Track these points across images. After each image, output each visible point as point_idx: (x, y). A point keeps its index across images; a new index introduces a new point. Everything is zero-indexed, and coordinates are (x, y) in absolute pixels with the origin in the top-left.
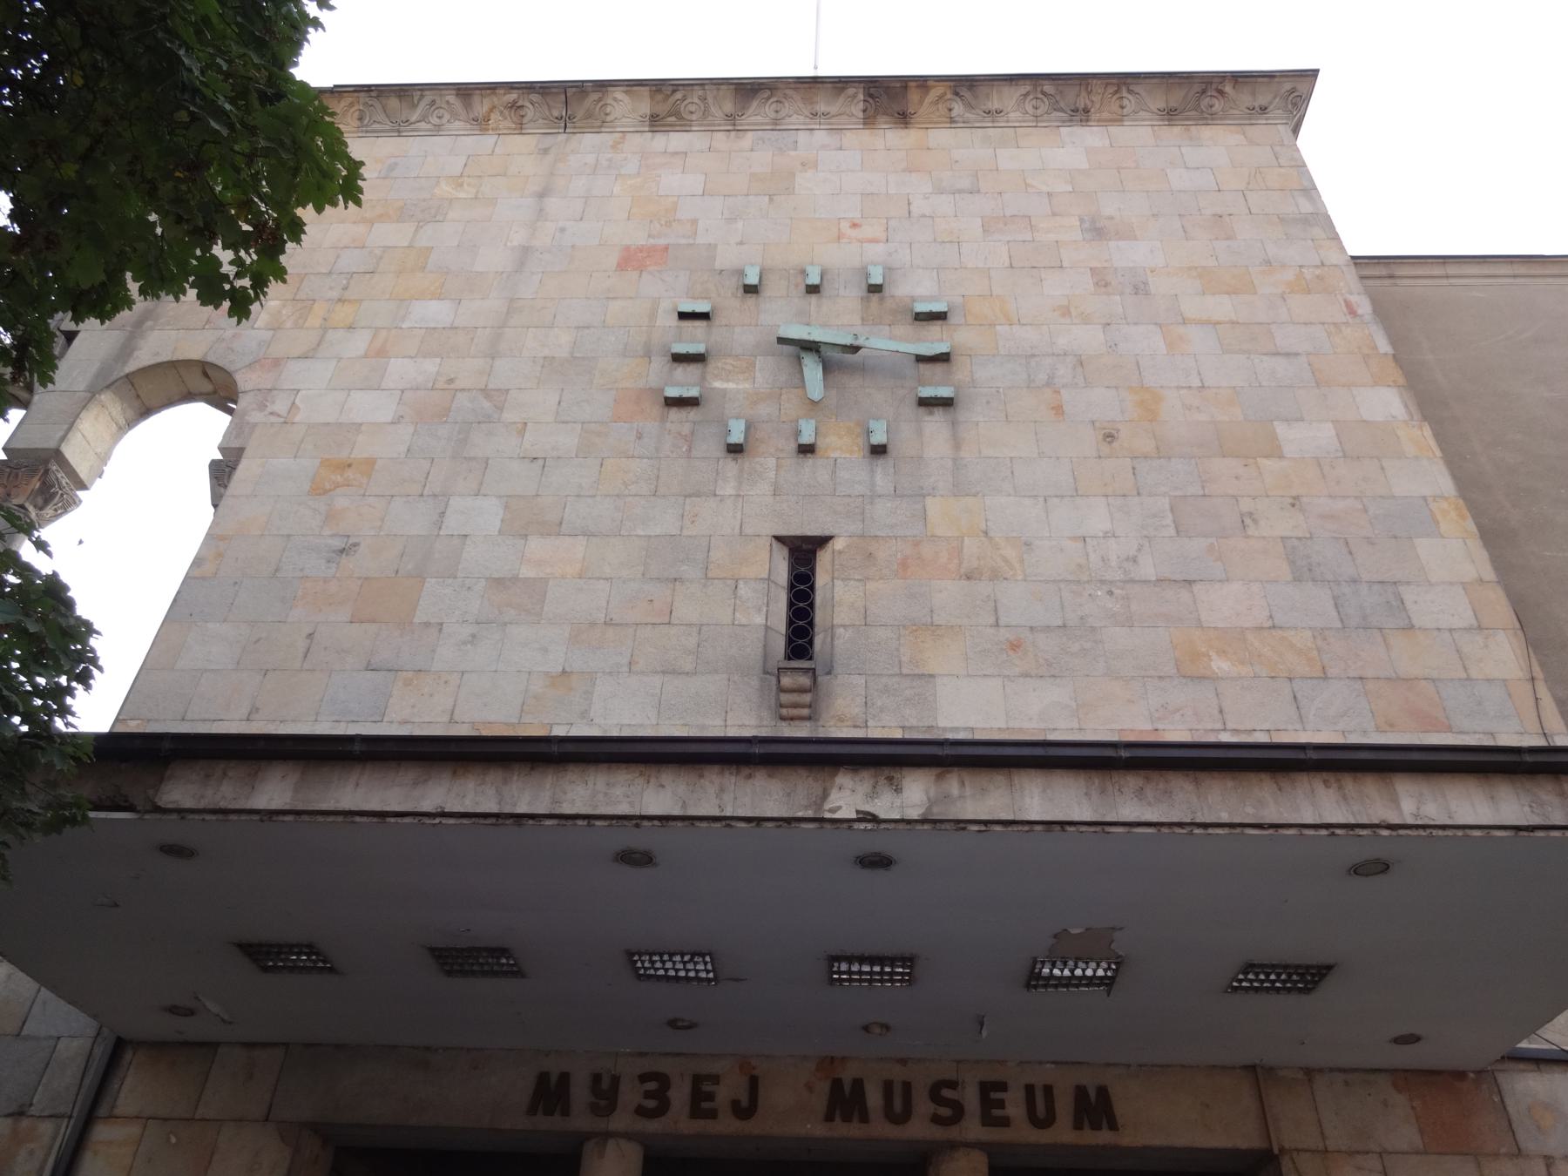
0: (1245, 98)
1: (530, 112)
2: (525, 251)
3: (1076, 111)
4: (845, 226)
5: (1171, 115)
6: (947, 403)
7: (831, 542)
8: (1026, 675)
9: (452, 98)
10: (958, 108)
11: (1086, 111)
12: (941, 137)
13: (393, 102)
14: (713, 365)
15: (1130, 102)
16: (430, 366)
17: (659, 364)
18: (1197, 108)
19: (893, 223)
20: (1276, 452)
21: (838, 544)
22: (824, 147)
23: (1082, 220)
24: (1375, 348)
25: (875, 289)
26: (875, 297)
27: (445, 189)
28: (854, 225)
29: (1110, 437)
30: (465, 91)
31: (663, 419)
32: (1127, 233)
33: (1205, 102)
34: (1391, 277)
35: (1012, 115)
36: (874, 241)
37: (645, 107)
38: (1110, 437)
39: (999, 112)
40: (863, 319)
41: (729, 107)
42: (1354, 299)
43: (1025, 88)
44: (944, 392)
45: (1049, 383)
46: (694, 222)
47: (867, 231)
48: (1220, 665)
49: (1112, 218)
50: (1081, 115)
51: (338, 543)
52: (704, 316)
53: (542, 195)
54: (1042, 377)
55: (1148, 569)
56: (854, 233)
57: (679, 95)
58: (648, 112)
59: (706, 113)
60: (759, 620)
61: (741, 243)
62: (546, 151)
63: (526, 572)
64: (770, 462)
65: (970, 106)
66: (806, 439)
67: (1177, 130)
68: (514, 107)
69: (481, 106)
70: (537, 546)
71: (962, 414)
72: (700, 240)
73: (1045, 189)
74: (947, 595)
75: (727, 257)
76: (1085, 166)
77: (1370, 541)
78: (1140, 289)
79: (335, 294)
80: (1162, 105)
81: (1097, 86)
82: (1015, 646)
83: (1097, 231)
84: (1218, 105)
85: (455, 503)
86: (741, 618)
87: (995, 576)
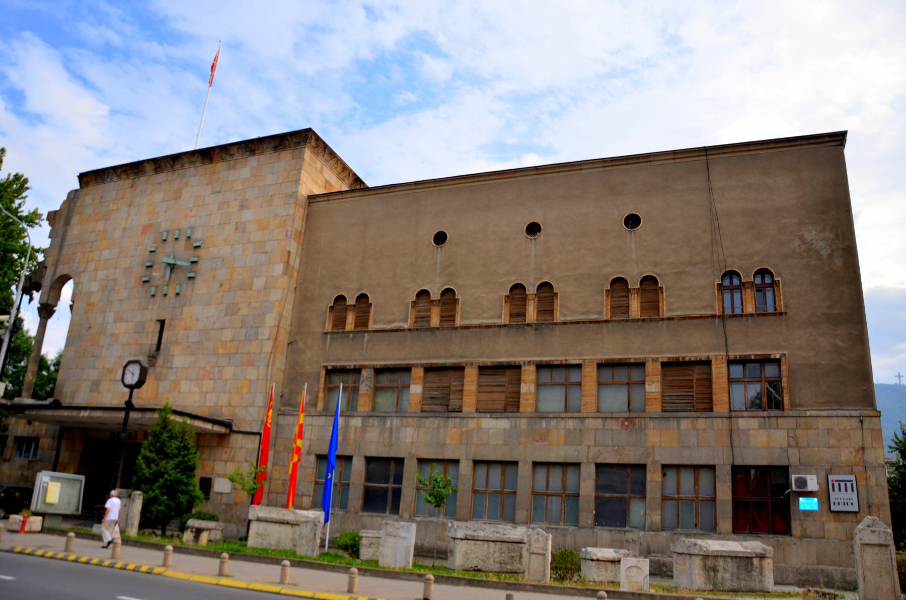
0: (295, 140)
1: (129, 172)
2: (125, 229)
3: (252, 151)
5: (275, 149)
6: (193, 278)
8: (189, 354)
9: (112, 171)
10: (224, 155)
11: (254, 151)
13: (100, 174)
14: (155, 267)
16: (105, 272)
17: (144, 268)
18: (281, 145)
20: (251, 289)
23: (240, 202)
24: (285, 248)
25: (189, 237)
29: (221, 285)
30: (115, 169)
31: (143, 287)
32: (248, 208)
33: (284, 143)
34: (328, 200)
35: (237, 155)
36: (193, 217)
37: (153, 166)
38: (221, 285)
39: (233, 154)
41: (171, 163)
42: (289, 228)
44: (192, 275)
45: (215, 268)
46: (158, 213)
48: (221, 351)
49: (247, 200)
50: (253, 152)
52: (154, 251)
53: (130, 206)
54: (214, 266)
55: (216, 326)
56: (190, 214)
57: (159, 162)
58: (153, 167)
59: (166, 167)
60: (150, 342)
61: (166, 221)
62: (132, 186)
63: (117, 332)
64: (158, 298)
65: (226, 154)
66: (165, 292)
67: (277, 153)
68: (125, 171)
69: (119, 172)
70: (119, 325)
72: (159, 221)
73: (236, 188)
74: (181, 333)
77: (259, 315)
78: (244, 231)
79: (89, 250)
80: (273, 145)
81: (255, 142)
82: (189, 347)
83: (242, 207)
84: (287, 143)
85: (108, 313)
86: (148, 342)
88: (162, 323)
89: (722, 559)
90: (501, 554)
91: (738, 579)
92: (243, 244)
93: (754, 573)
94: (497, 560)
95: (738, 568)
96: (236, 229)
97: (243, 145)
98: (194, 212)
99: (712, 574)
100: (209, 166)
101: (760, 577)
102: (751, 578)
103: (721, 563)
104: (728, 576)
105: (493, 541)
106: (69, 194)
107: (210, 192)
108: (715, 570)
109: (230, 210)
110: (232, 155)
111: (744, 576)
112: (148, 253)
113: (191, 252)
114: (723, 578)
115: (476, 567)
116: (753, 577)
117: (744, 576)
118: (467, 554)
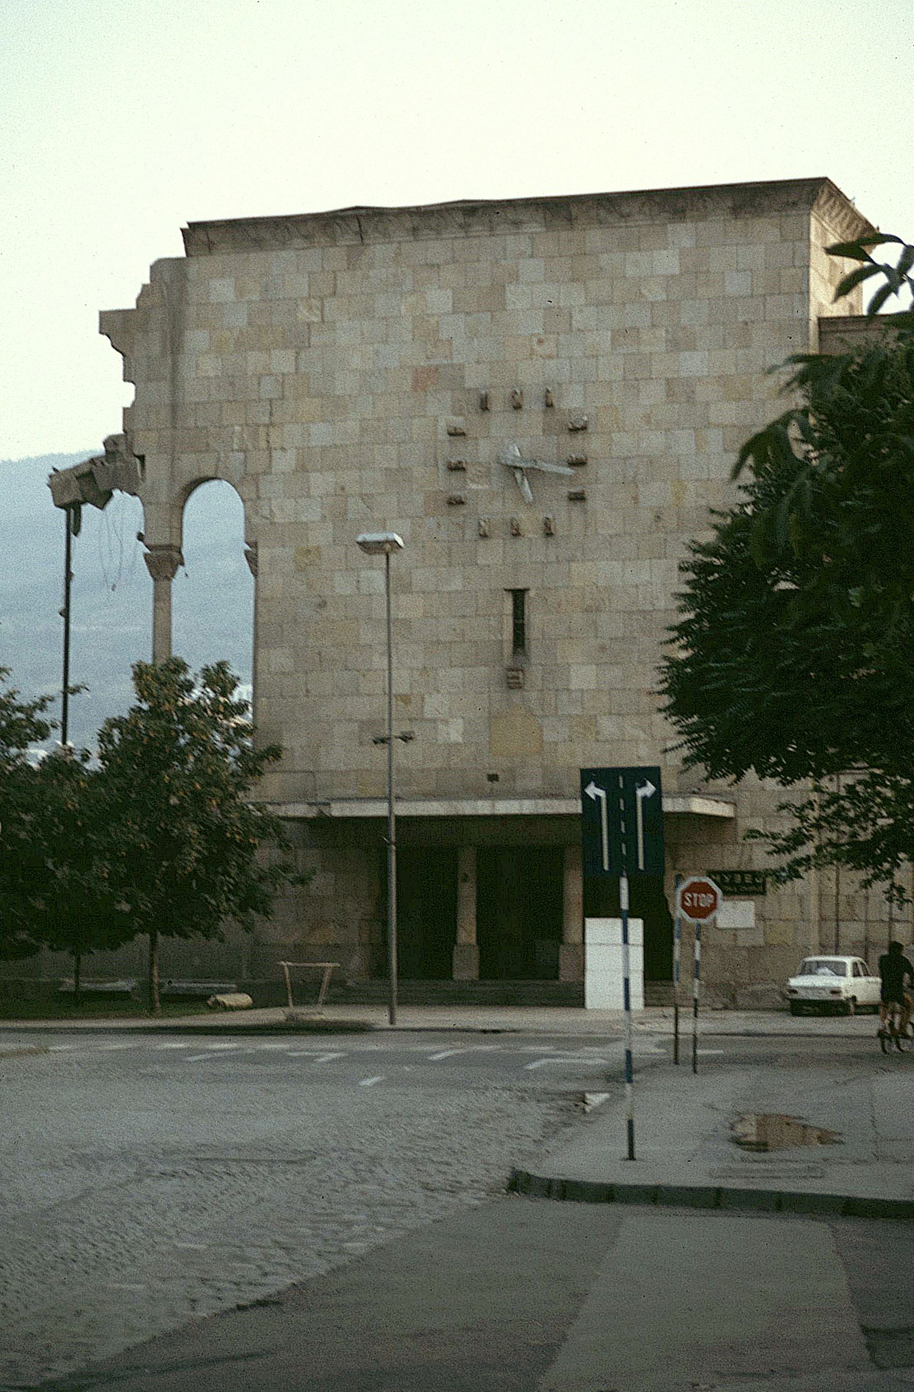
4: (535, 340)
5: (736, 211)
7: (527, 593)
10: (603, 213)
11: (684, 211)
12: (595, 237)
15: (710, 205)
16: (330, 477)
19: (561, 338)
21: (532, 593)
22: (521, 255)
26: (549, 409)
27: (303, 314)
28: (540, 342)
36: (550, 357)
40: (544, 430)
43: (643, 199)
46: (450, 341)
47: (548, 348)
49: (684, 328)
51: (318, 600)
67: (740, 223)
71: (590, 504)
75: (472, 382)
76: (677, 271)
78: (690, 399)
82: (603, 648)
87: (598, 610)
88: (519, 596)
92: (695, 429)
96: (670, 393)
97: (657, 199)
98: (548, 348)
100: (564, 235)
106: (158, 268)
107: (582, 301)
109: (646, 349)
110: (625, 216)
112: (443, 436)
113: (565, 438)
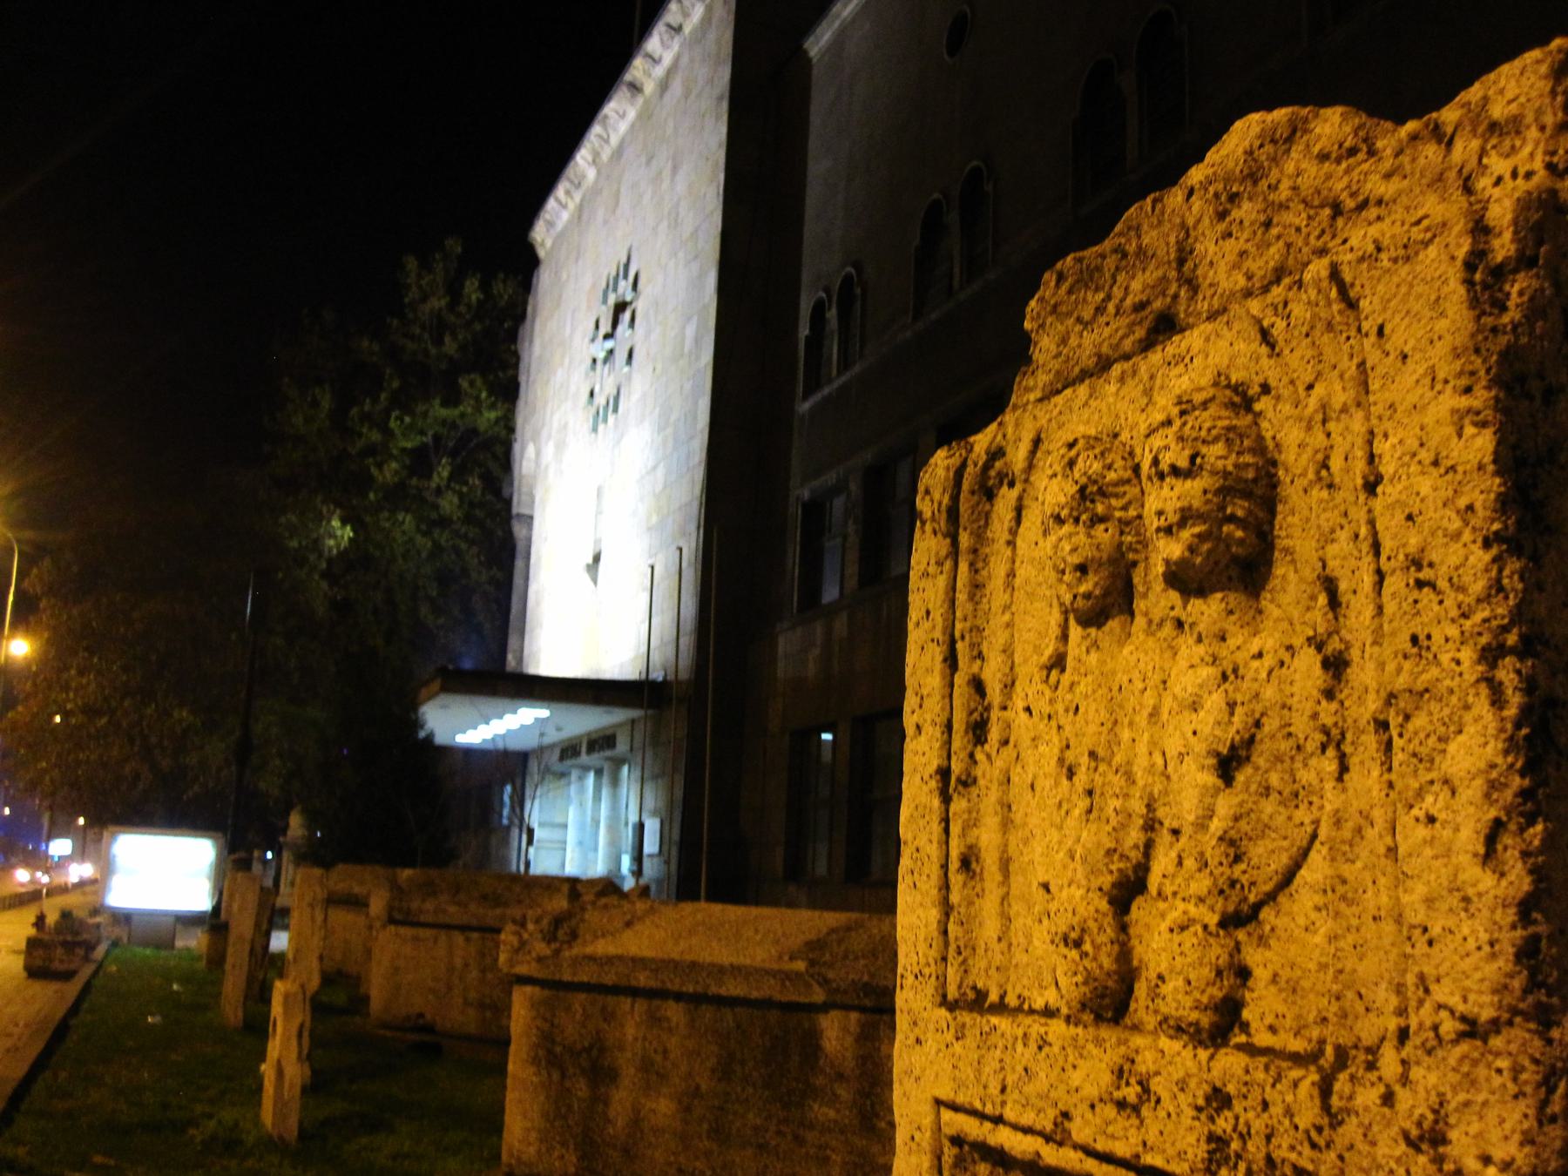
89: (641, 1006)
90: (483, 971)
91: (719, 1133)
93: (822, 1112)
94: (473, 995)
95: (724, 1071)
99: (581, 1089)
101: (859, 1142)
102: (799, 1140)
103: (631, 1024)
104: (663, 1108)
105: (464, 928)
108: (601, 1074)
111: (753, 1118)
114: (636, 1122)
115: (421, 1015)
116: (811, 1136)
117: (753, 1118)
118: (397, 969)
